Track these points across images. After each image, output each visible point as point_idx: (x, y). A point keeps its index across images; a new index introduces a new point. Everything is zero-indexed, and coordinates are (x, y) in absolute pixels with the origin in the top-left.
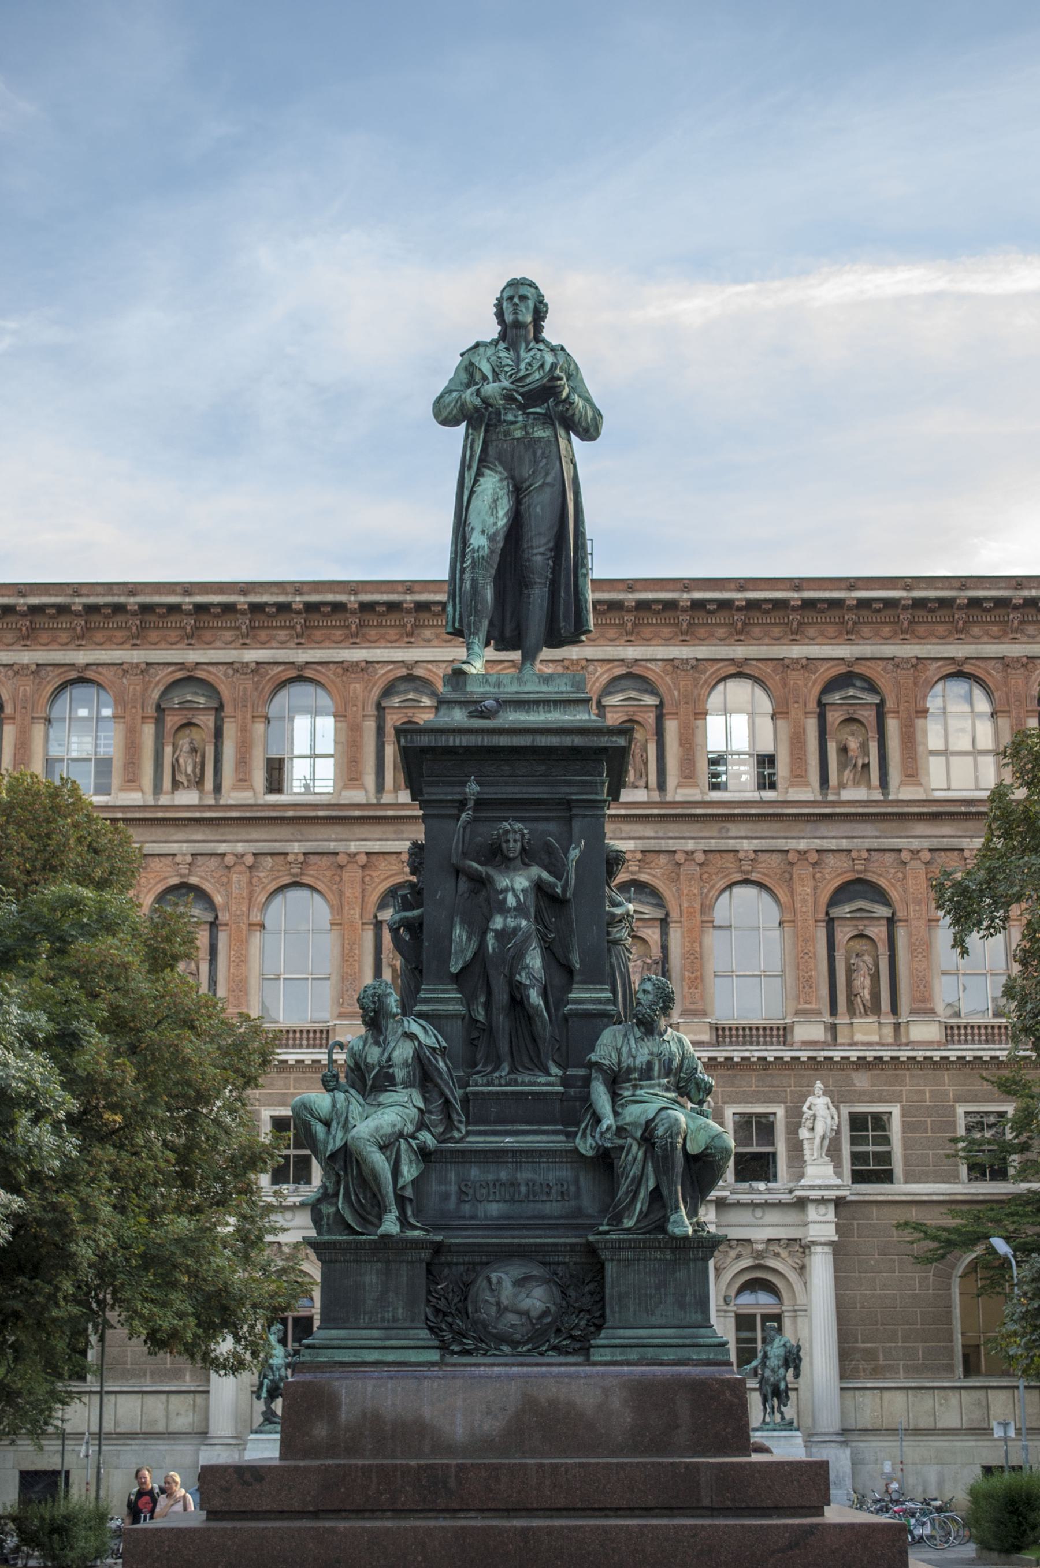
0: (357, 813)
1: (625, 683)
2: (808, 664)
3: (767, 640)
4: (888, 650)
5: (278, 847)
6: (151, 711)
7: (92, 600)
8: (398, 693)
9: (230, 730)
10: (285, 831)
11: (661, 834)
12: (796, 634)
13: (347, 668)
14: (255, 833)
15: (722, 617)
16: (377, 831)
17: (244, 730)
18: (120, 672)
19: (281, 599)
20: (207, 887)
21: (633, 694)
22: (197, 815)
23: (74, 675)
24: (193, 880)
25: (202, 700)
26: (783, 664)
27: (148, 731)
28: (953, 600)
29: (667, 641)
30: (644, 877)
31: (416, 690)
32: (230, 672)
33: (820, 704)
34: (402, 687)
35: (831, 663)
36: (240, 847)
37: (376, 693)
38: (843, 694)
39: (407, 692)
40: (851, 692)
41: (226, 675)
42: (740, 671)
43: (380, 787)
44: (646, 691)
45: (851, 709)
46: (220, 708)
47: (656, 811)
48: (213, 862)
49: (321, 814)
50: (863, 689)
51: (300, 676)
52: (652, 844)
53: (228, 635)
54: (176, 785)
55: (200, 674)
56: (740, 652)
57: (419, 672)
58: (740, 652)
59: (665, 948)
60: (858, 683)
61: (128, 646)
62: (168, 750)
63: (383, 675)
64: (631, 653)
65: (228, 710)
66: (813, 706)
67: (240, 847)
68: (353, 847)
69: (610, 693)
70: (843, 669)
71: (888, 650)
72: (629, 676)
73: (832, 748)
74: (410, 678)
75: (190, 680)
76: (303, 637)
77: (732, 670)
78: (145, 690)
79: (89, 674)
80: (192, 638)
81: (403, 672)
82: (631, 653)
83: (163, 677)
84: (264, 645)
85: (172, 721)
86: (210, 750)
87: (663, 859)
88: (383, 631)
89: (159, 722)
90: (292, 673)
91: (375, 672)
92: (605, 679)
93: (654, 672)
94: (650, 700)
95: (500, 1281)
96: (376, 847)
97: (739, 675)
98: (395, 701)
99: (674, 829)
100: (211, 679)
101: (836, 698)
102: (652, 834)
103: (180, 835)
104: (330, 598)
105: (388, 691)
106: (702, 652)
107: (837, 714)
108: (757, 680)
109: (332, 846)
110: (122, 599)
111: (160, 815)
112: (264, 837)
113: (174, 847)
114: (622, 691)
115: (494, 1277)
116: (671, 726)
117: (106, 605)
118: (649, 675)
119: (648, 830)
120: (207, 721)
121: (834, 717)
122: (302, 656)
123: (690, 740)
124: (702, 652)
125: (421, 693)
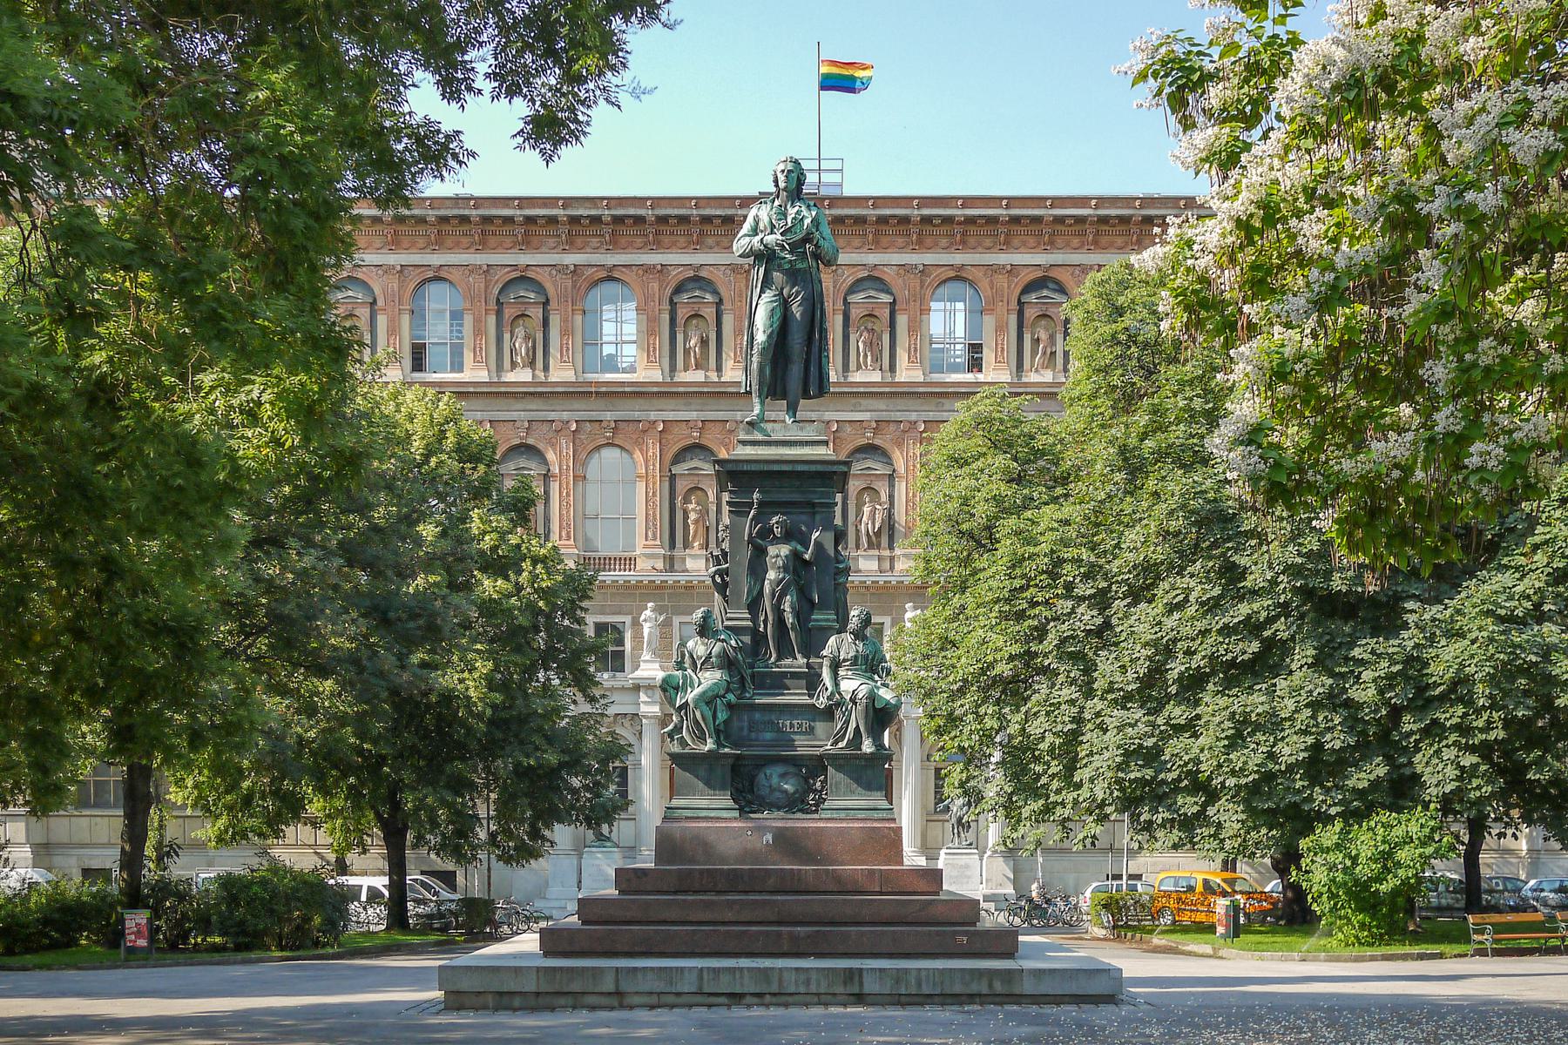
0: (655, 389)
1: (867, 284)
2: (1013, 270)
3: (980, 250)
4: (1076, 258)
5: (594, 415)
6: (493, 306)
7: (443, 212)
8: (687, 291)
9: (555, 320)
10: (601, 403)
11: (891, 408)
12: (1007, 245)
13: (647, 269)
14: (577, 404)
15: (944, 229)
16: (672, 403)
17: (565, 320)
18: (467, 272)
19: (593, 212)
20: (541, 446)
21: (872, 293)
22: (532, 390)
23: (430, 274)
24: (530, 441)
25: (532, 295)
26: (993, 269)
27: (492, 319)
28: (1131, 217)
29: (901, 249)
30: (877, 442)
31: (700, 289)
32: (554, 272)
33: (1019, 302)
34: (690, 286)
35: (1031, 269)
36: (565, 416)
37: (669, 291)
38: (1038, 294)
39: (693, 289)
40: (1045, 292)
41: (550, 274)
42: (959, 276)
43: (673, 368)
44: (882, 291)
45: (1044, 307)
46: (546, 303)
47: (887, 390)
48: (545, 427)
49: (627, 389)
50: (1055, 290)
51: (610, 276)
52: (884, 416)
53: (551, 242)
54: (514, 365)
55: (530, 274)
56: (958, 258)
57: (703, 274)
58: (958, 258)
59: (891, 497)
60: (1051, 285)
61: (472, 250)
62: (507, 336)
63: (675, 277)
64: (872, 259)
65: (553, 304)
66: (1014, 305)
67: (565, 416)
68: (653, 416)
69: (854, 292)
70: (1040, 274)
71: (1076, 258)
72: (870, 278)
73: (1027, 338)
74: (697, 279)
75: (523, 279)
76: (614, 244)
77: (952, 274)
78: (486, 287)
79: (443, 274)
80: (526, 243)
81: (691, 273)
82: (872, 259)
83: (502, 276)
84: (581, 250)
85: (509, 313)
86: (539, 336)
87: (892, 427)
88: (674, 238)
89: (499, 313)
90: (603, 274)
91: (669, 271)
92: (850, 280)
93: (889, 275)
94: (887, 298)
95: (771, 775)
96: (670, 416)
97: (958, 278)
98: (684, 297)
99: (900, 403)
100: (539, 278)
101: (1032, 297)
102: (884, 408)
103: (519, 406)
104: (632, 211)
105: (678, 290)
106: (929, 258)
107: (1033, 311)
108: (972, 284)
109: (637, 415)
110: (466, 212)
111: (503, 389)
112: (584, 407)
113: (514, 415)
114: (864, 290)
115: (768, 772)
116: (902, 320)
117: (454, 217)
118: (885, 277)
119: (880, 404)
120: (536, 313)
121: (1031, 313)
122: (611, 259)
123: (916, 327)
124: (929, 258)
125: (705, 290)
